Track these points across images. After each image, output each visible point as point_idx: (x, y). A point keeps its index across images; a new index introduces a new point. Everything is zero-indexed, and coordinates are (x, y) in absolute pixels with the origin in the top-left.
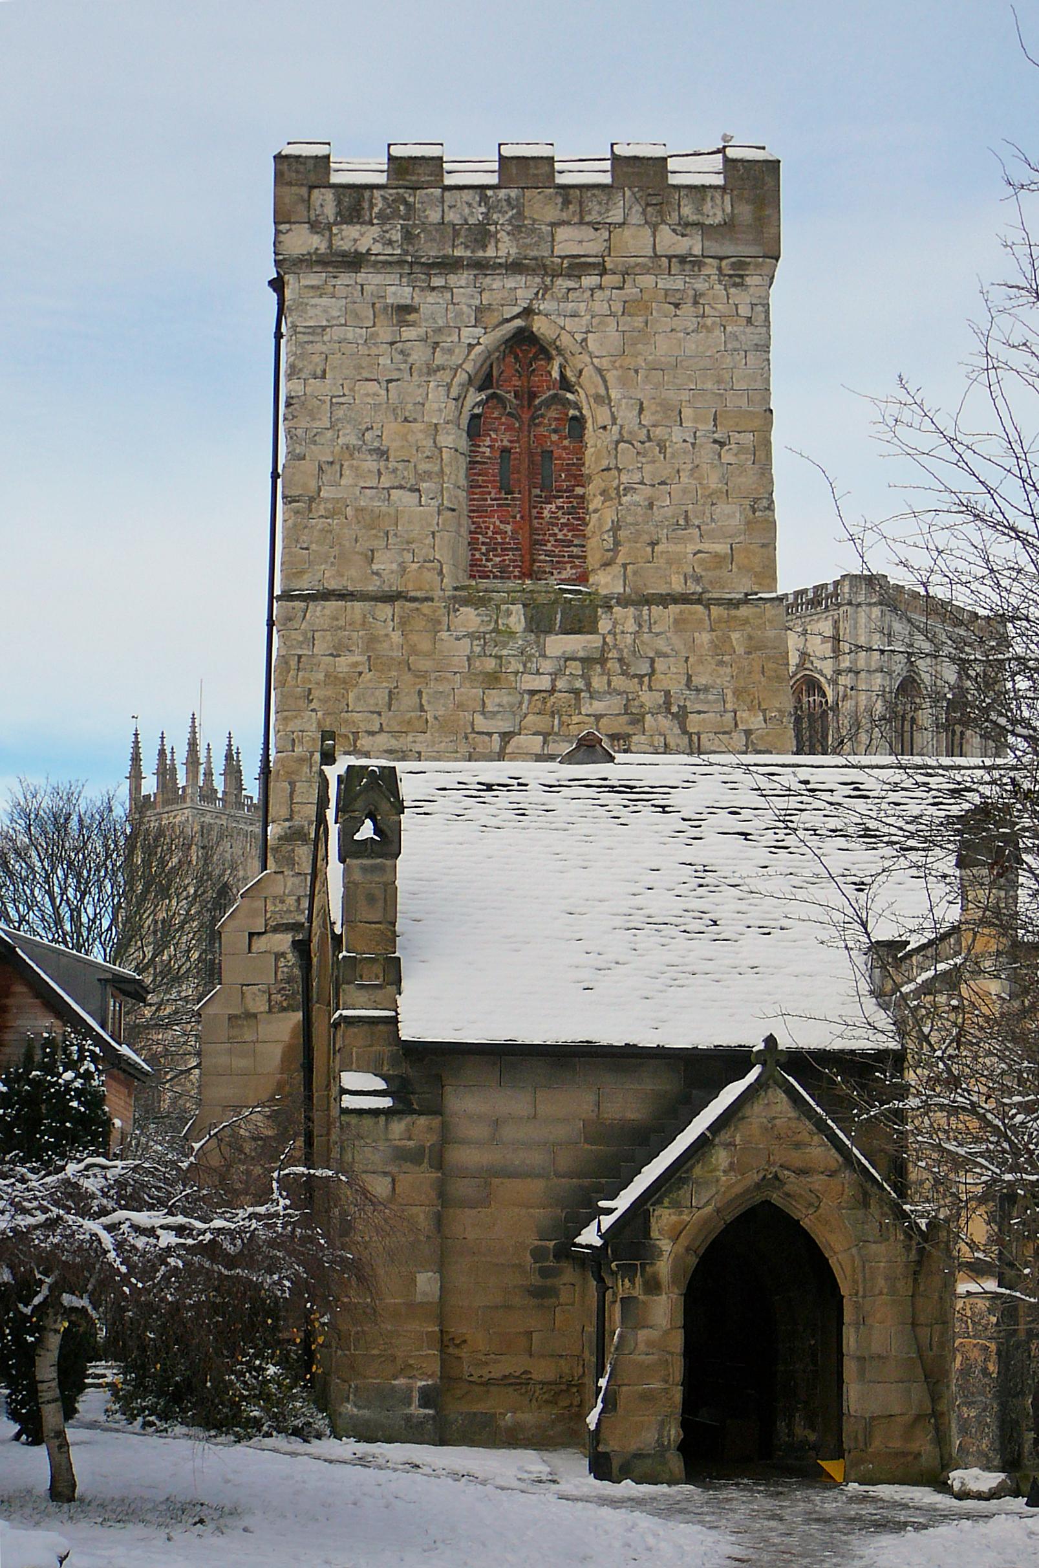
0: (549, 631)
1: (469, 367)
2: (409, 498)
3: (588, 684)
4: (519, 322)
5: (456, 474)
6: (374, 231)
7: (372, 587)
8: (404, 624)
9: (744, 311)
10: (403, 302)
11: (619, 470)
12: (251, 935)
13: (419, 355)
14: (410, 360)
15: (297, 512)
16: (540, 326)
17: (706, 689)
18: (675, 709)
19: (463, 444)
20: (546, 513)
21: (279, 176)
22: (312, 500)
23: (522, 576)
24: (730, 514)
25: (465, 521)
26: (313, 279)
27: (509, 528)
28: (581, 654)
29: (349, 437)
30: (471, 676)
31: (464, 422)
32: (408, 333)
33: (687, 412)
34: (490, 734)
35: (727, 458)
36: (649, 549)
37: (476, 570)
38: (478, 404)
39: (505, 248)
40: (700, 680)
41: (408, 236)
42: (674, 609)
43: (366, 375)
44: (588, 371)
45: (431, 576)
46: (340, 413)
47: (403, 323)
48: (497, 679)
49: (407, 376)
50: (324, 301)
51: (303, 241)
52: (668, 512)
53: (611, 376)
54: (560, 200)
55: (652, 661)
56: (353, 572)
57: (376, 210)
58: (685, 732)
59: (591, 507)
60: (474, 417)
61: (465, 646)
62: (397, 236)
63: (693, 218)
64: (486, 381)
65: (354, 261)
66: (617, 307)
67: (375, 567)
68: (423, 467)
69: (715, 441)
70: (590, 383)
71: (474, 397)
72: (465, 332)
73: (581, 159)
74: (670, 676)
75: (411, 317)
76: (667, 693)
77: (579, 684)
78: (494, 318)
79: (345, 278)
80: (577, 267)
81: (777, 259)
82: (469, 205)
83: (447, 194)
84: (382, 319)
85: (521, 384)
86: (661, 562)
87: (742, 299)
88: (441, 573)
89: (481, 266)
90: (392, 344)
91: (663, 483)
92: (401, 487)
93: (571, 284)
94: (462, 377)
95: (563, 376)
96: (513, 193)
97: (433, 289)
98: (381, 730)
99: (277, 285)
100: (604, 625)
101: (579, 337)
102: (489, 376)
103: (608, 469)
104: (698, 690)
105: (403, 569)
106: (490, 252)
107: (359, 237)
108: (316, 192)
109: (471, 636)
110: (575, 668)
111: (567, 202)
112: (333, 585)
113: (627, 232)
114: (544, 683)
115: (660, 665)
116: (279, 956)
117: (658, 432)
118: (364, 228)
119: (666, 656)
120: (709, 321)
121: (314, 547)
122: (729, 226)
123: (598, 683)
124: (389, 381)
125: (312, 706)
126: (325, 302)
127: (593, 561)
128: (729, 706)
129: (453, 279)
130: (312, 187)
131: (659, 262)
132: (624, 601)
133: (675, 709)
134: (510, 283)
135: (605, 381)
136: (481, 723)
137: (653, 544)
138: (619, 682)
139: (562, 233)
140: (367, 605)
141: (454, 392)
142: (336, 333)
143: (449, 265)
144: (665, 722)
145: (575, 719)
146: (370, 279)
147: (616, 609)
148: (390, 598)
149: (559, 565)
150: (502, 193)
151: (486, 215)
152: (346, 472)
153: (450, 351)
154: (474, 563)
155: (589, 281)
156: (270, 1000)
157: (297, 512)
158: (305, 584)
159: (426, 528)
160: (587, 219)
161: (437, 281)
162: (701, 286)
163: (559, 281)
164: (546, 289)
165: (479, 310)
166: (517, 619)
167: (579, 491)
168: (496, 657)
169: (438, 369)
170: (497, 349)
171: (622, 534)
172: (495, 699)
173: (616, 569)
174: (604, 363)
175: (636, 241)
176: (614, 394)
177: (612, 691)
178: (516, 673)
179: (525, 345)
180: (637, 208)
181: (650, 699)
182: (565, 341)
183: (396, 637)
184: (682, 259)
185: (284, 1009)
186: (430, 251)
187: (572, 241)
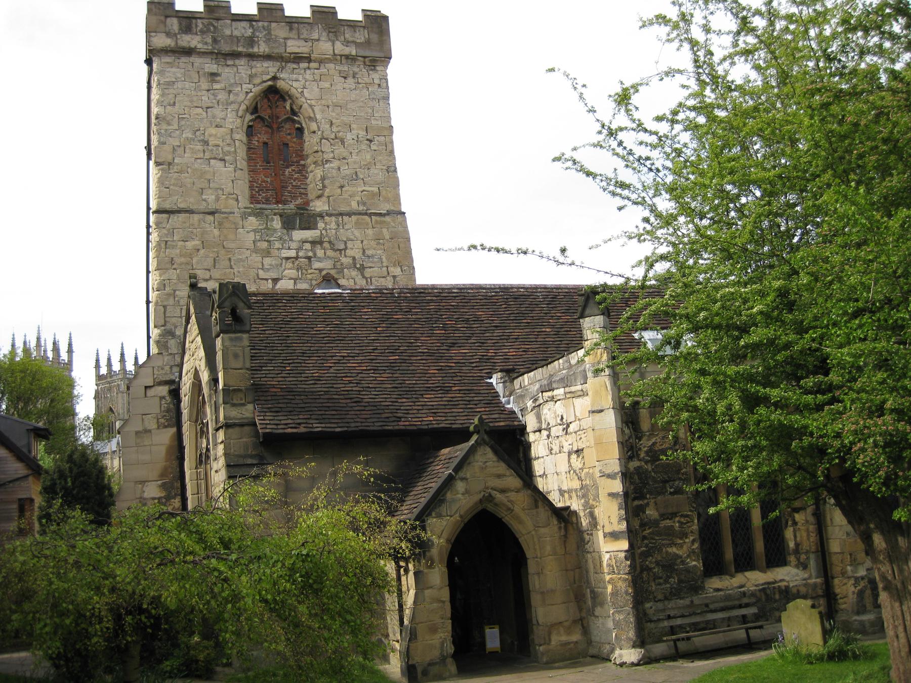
0: (294, 229)
1: (246, 102)
2: (221, 164)
3: (315, 254)
4: (270, 83)
5: (242, 153)
6: (198, 38)
7: (202, 206)
9: (377, 81)
10: (213, 71)
11: (323, 152)
13: (222, 96)
14: (217, 98)
15: (162, 170)
16: (280, 84)
17: (373, 256)
18: (358, 266)
19: (244, 139)
20: (287, 173)
21: (149, 10)
22: (170, 164)
23: (277, 202)
24: (377, 173)
25: (247, 176)
27: (269, 180)
28: (310, 239)
29: (188, 134)
30: (256, 250)
31: (245, 128)
32: (216, 86)
34: (267, 280)
36: (339, 190)
37: (253, 199)
38: (251, 121)
39: (262, 48)
41: (215, 41)
42: (354, 218)
43: (195, 105)
44: (305, 106)
45: (232, 202)
46: (183, 123)
47: (213, 81)
48: (269, 252)
49: (216, 106)
50: (174, 70)
51: (162, 41)
52: (347, 172)
53: (316, 109)
54: (288, 28)
55: (346, 243)
56: (192, 200)
58: (364, 277)
59: (309, 170)
60: (249, 127)
61: (251, 236)
62: (209, 40)
63: (351, 39)
64: (254, 110)
65: (188, 52)
67: (204, 197)
68: (227, 149)
70: (306, 110)
71: (249, 117)
72: (244, 86)
74: (354, 251)
75: (218, 78)
76: (354, 258)
77: (310, 254)
78: (257, 81)
79: (184, 59)
80: (297, 59)
81: (390, 58)
82: (244, 28)
83: (234, 23)
84: (202, 79)
86: (346, 196)
87: (375, 76)
88: (237, 200)
89: (252, 56)
90: (208, 90)
91: (344, 158)
92: (215, 158)
93: (295, 66)
94: (243, 107)
95: (292, 109)
96: (266, 24)
98: (211, 278)
99: (149, 62)
100: (321, 225)
101: (300, 90)
103: (317, 152)
104: (369, 257)
105: (218, 199)
106: (256, 50)
107: (188, 40)
108: (168, 20)
109: (255, 231)
110: (308, 246)
111: (291, 29)
112: (182, 205)
113: (321, 43)
114: (292, 253)
115: (350, 244)
118: (193, 37)
119: (352, 240)
120: (361, 86)
121: (171, 187)
122: (368, 43)
123: (320, 253)
124: (207, 108)
125: (174, 267)
126: (176, 70)
127: (311, 197)
128: (385, 264)
129: (237, 62)
130: (166, 17)
131: (337, 58)
132: (330, 215)
133: (358, 266)
134: (266, 64)
135: (313, 111)
136: (262, 274)
137: (342, 187)
138: (330, 253)
139: (289, 43)
140: (201, 216)
141: (240, 113)
142: (180, 85)
143: (235, 55)
144: (354, 273)
145: (310, 271)
146: (197, 60)
147: (326, 218)
148: (212, 213)
149: (294, 198)
150: (260, 24)
151: (253, 33)
152: (187, 151)
153: (237, 95)
155: (304, 65)
158: (167, 206)
159: (229, 178)
161: (230, 62)
162: (356, 69)
163: (289, 65)
164: (283, 68)
165: (251, 77)
166: (277, 223)
167: (302, 162)
168: (267, 241)
169: (232, 103)
171: (326, 182)
172: (267, 261)
173: (324, 199)
174: (313, 102)
175: (325, 47)
176: (318, 117)
177: (326, 257)
178: (278, 249)
179: (273, 94)
180: (324, 34)
182: (293, 91)
183: (216, 232)
184: (347, 57)
186: (226, 48)
187: (295, 46)
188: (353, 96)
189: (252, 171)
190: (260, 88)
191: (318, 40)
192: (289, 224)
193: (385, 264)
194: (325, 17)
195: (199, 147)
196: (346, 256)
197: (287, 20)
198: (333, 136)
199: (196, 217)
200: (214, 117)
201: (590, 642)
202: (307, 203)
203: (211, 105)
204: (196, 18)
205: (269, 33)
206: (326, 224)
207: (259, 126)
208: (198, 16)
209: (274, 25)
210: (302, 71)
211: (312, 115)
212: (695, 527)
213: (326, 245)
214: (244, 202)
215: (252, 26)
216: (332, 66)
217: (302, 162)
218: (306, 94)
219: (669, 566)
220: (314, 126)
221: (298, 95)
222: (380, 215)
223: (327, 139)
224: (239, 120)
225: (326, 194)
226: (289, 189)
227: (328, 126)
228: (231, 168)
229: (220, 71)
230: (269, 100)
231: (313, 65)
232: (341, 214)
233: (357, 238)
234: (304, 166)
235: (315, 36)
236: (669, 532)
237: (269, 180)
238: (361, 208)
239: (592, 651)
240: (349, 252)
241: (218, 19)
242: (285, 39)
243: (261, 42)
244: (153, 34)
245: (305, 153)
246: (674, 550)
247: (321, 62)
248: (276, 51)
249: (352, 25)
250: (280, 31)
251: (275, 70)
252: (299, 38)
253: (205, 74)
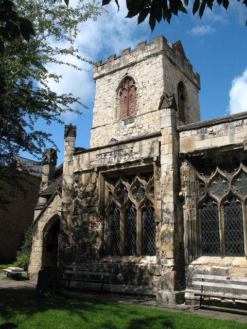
6: (105, 70)
8: (107, 129)
16: (129, 75)
26: (98, 80)
39: (122, 65)
47: (109, 82)
61: (115, 130)
65: (102, 76)
100: (136, 120)
110: (131, 129)
114: (126, 133)
138: (138, 130)
143: (115, 71)
146: (105, 77)
175: (141, 56)
179: (128, 79)
186: (112, 70)
187: (132, 60)
188: (150, 70)
231: (138, 64)
235: (137, 54)
238: (150, 110)
240: (144, 128)
247: (140, 62)
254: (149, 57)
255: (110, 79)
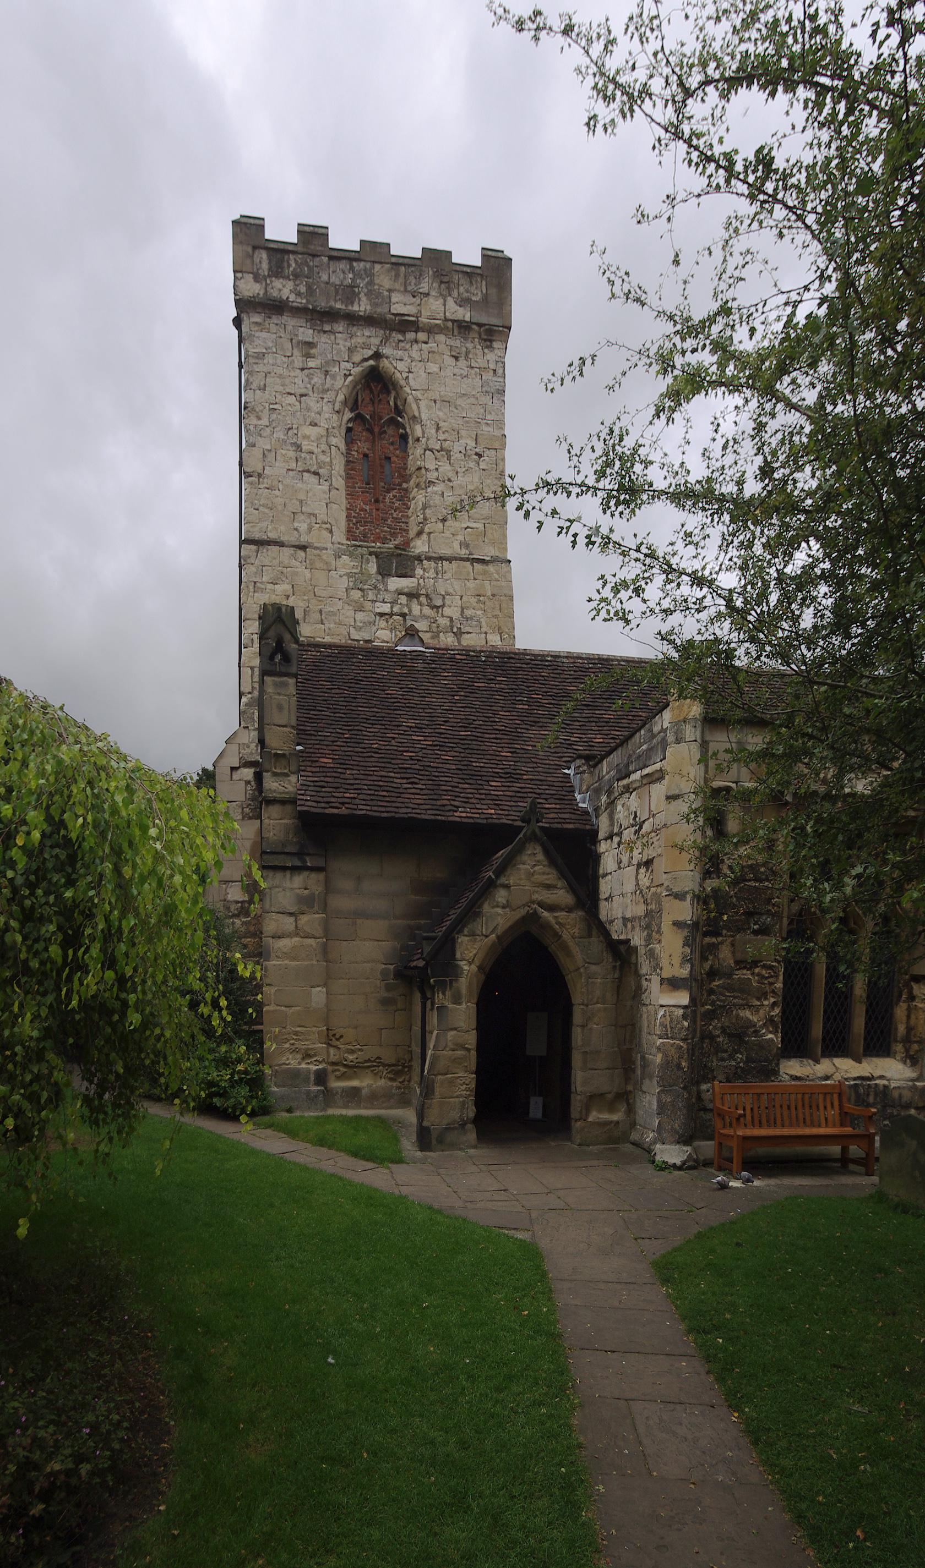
2: (314, 479)
3: (410, 611)
4: (371, 362)
6: (290, 285)
10: (307, 340)
11: (427, 470)
12: (233, 769)
13: (317, 379)
14: (313, 382)
15: (251, 483)
17: (471, 618)
18: (455, 630)
19: (343, 446)
22: (260, 475)
26: (257, 318)
28: (406, 590)
31: (343, 431)
32: (311, 363)
33: (463, 433)
35: (483, 466)
36: (441, 525)
37: (350, 534)
38: (350, 420)
39: (362, 306)
40: (468, 613)
43: (288, 390)
46: (274, 416)
47: (308, 356)
49: (311, 393)
53: (423, 404)
55: (444, 598)
56: (282, 528)
57: (291, 269)
62: (303, 289)
66: (425, 356)
67: (296, 525)
69: (477, 454)
71: (348, 415)
73: (406, 246)
75: (313, 351)
76: (451, 619)
77: (406, 610)
78: (357, 358)
83: (331, 263)
85: (376, 411)
86: (448, 534)
88: (331, 532)
89: (353, 319)
90: (302, 369)
91: (449, 480)
92: (308, 471)
94: (341, 397)
96: (368, 265)
97: (325, 332)
100: (419, 572)
101: (405, 375)
102: (356, 401)
103: (419, 469)
104: (467, 619)
106: (356, 308)
107: (284, 289)
108: (257, 252)
110: (403, 599)
112: (272, 535)
114: (386, 608)
116: (248, 782)
117: (446, 445)
121: (261, 509)
124: (302, 396)
130: (255, 248)
132: (429, 559)
133: (455, 630)
138: (427, 611)
140: (292, 550)
142: (269, 359)
146: (290, 322)
147: (425, 562)
148: (303, 548)
149: (394, 535)
151: (353, 279)
152: (278, 458)
154: (349, 531)
155: (411, 335)
156: (243, 812)
157: (251, 483)
158: (257, 536)
159: (324, 502)
160: (409, 288)
163: (394, 334)
165: (351, 350)
166: (372, 567)
168: (361, 590)
170: (360, 380)
172: (360, 616)
174: (418, 394)
176: (424, 417)
177: (424, 617)
178: (373, 601)
181: (443, 622)
185: (250, 818)
186: (322, 304)
187: (401, 305)
189: (350, 495)
190: (359, 369)
191: (427, 295)
192: (384, 573)
193: (484, 630)
194: (436, 260)
195: (292, 454)
196: (443, 616)
197: (393, 260)
198: (438, 447)
199: (287, 551)
200: (308, 409)
201: (633, 1125)
202: (407, 543)
203: (304, 391)
204: (289, 252)
205: (371, 283)
206: (424, 570)
207: (358, 429)
208: (291, 248)
209: (377, 267)
210: (408, 346)
211: (417, 414)
212: (779, 985)
213: (423, 599)
214: (340, 536)
215: (352, 269)
216: (441, 338)
217: (405, 485)
218: (412, 382)
219: (739, 1034)
220: (418, 432)
221: (403, 383)
222: (482, 561)
223: (431, 450)
224: (335, 417)
225: (427, 530)
226: (389, 522)
227: (433, 431)
228: (325, 487)
229: (316, 340)
230: (371, 391)
232: (441, 558)
233: (454, 586)
234: (406, 490)
235: (424, 287)
236: (743, 989)
237: (367, 508)
239: (634, 1136)
241: (314, 256)
242: (390, 291)
243: (362, 295)
244: (239, 275)
245: (408, 472)
246: (746, 1014)
248: (379, 310)
249: (469, 273)
250: (384, 280)
251: (377, 341)
252: (406, 290)
253: (298, 342)
254: (463, 327)
255: (310, 345)
